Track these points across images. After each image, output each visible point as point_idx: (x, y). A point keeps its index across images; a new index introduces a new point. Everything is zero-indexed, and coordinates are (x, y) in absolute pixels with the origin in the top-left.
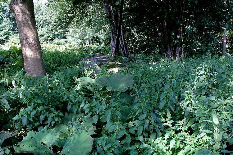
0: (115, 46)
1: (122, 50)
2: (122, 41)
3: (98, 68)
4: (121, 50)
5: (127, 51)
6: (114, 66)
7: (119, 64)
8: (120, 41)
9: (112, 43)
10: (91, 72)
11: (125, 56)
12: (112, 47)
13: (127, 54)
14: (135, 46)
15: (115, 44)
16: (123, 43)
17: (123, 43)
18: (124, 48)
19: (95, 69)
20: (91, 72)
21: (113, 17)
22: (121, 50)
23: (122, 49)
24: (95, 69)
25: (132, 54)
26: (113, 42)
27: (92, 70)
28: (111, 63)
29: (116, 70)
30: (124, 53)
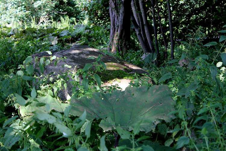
0: (119, 22)
1: (140, 34)
2: (139, 9)
3: (74, 75)
4: (137, 33)
5: (152, 38)
6: (120, 75)
7: (132, 70)
8: (133, 9)
9: (113, 14)
10: (56, 90)
11: (148, 50)
12: (111, 27)
13: (153, 46)
14: (176, 23)
15: (121, 17)
16: (143, 15)
17: (143, 15)
18: (146, 28)
19: (66, 79)
20: (56, 90)
21: (184, 92)
22: (137, 33)
23: (140, 31)
24: (66, 79)
25: (167, 45)
26: (115, 13)
27: (59, 83)
28: (111, 66)
29: (123, 84)
30: (145, 43)
